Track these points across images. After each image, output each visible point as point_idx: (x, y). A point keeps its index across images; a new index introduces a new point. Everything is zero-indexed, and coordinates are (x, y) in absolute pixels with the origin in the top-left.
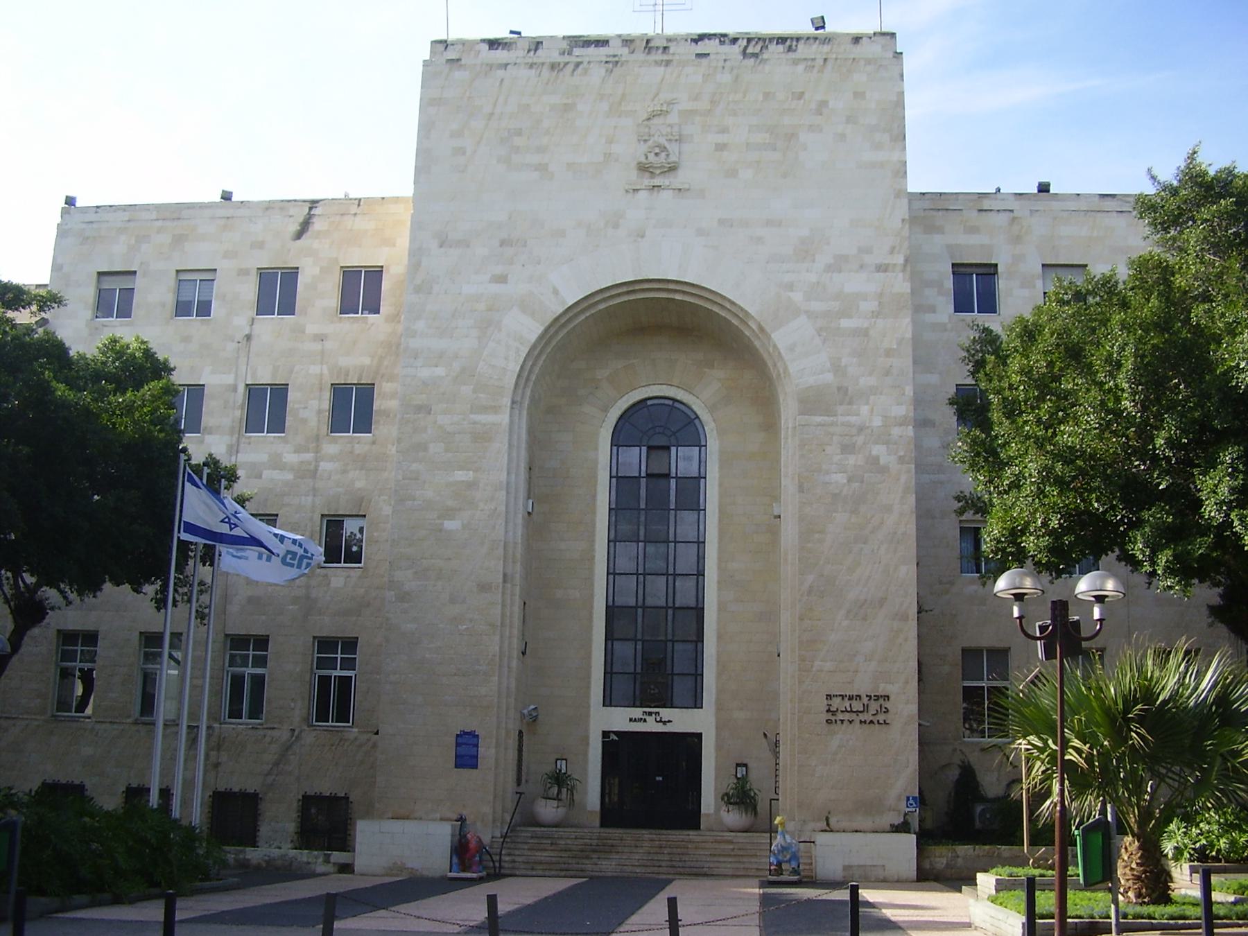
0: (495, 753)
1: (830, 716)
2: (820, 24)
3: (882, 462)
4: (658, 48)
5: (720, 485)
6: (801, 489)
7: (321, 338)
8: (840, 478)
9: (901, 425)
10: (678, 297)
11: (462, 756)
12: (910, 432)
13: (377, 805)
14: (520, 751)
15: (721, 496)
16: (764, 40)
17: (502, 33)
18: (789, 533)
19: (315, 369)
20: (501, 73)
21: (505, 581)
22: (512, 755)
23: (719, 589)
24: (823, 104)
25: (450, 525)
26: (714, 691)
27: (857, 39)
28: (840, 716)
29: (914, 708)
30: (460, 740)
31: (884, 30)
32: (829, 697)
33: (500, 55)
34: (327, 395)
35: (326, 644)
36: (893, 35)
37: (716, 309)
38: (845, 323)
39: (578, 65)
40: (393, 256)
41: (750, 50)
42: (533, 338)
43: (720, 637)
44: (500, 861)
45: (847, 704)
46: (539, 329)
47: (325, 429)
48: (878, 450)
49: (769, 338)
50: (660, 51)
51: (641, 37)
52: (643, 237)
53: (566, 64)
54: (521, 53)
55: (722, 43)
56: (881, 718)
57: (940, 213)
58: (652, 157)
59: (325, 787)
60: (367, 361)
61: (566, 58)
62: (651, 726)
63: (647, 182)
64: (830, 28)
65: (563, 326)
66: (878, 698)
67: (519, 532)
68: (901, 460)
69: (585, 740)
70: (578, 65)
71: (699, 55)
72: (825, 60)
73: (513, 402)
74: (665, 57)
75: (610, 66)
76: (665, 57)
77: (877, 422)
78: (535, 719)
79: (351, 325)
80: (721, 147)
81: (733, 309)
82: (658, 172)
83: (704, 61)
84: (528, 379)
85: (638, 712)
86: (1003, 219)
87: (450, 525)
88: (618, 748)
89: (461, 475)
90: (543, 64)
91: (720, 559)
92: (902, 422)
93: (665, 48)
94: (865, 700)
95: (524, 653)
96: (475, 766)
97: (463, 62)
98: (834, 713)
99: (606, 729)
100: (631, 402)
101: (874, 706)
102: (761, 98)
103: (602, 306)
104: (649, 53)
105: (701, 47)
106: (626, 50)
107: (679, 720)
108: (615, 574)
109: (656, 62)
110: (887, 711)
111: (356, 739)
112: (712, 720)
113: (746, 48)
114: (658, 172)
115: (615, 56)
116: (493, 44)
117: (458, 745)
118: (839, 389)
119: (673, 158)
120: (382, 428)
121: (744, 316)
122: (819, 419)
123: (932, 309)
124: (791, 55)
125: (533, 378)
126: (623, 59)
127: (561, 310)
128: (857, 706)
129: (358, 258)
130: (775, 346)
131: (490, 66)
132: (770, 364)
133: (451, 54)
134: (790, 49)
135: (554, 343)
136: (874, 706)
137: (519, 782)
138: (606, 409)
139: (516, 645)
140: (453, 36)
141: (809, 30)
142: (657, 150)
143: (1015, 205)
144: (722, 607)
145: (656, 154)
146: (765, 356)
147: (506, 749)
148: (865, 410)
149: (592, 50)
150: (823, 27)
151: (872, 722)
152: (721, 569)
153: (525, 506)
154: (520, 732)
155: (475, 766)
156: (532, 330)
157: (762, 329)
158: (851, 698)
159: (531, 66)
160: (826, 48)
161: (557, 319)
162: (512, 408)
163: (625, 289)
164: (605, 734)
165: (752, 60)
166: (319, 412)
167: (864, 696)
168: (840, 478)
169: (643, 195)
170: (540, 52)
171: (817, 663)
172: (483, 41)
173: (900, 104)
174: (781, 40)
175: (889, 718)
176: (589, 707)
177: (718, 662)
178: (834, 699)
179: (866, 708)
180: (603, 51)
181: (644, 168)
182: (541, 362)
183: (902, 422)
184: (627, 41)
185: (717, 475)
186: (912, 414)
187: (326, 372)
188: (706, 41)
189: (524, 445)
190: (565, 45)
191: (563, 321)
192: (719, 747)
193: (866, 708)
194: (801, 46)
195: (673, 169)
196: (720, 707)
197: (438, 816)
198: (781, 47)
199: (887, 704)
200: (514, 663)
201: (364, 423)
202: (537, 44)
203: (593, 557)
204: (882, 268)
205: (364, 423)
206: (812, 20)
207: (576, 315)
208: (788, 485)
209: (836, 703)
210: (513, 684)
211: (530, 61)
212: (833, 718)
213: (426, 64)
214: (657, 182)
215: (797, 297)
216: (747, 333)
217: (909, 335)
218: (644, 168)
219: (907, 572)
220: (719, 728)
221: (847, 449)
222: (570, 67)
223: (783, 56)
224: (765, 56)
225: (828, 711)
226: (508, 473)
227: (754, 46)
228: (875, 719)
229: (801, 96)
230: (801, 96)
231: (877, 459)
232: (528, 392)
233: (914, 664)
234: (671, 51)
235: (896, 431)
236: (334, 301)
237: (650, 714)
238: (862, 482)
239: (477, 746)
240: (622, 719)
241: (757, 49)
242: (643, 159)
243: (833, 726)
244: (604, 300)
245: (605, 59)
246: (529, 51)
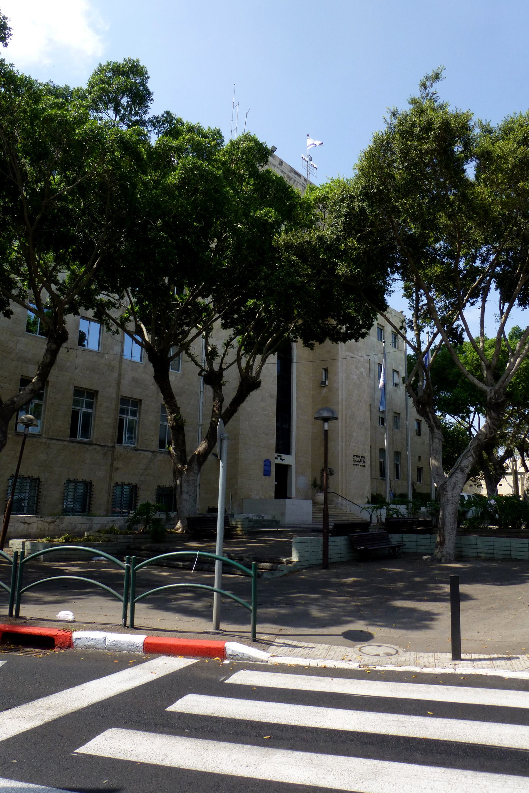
8: (355, 377)
13: (239, 492)
15: (298, 372)
28: (356, 463)
32: (354, 456)
43: (297, 428)
48: (362, 370)
56: (364, 464)
117: (265, 465)
144: (298, 415)
158: (359, 457)
192: (297, 472)
196: (297, 457)
220: (297, 463)
231: (362, 373)
239: (270, 466)
243: (355, 466)
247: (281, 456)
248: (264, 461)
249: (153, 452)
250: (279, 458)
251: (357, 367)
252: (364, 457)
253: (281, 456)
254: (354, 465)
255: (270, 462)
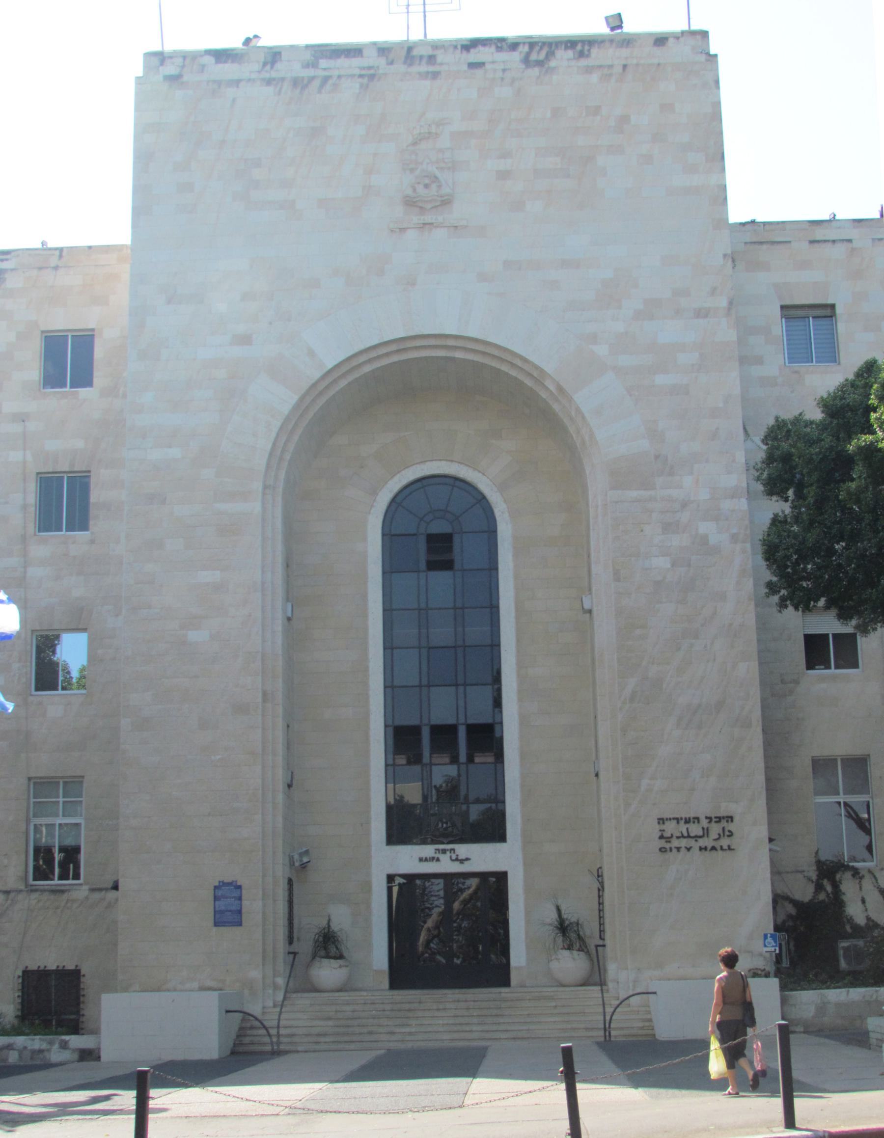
0: (262, 908)
1: (662, 844)
2: (616, 22)
3: (713, 540)
4: (421, 57)
5: (516, 577)
6: (617, 577)
7: (22, 418)
8: (662, 563)
9: (732, 497)
10: (459, 355)
11: (222, 912)
12: (743, 504)
14: (290, 903)
16: (550, 44)
17: (235, 43)
18: (605, 630)
19: (16, 456)
20: (231, 92)
21: (265, 700)
22: (282, 907)
23: (520, 700)
24: (624, 119)
25: (194, 636)
26: (519, 821)
27: (661, 40)
29: (762, 831)
30: (219, 893)
31: (693, 28)
32: (661, 821)
33: (229, 70)
34: (32, 487)
35: (42, 786)
36: (704, 34)
37: (504, 368)
38: (660, 380)
39: (326, 79)
40: (108, 318)
41: (534, 57)
42: (286, 409)
43: (523, 756)
44: (278, 1035)
45: (683, 828)
46: (296, 398)
47: (31, 528)
48: (706, 528)
49: (570, 400)
50: (424, 61)
51: (400, 45)
52: (414, 284)
53: (312, 79)
54: (256, 67)
55: (499, 49)
57: (765, 247)
58: (421, 190)
59: (50, 959)
60: (80, 444)
61: (311, 72)
62: (446, 866)
63: (416, 219)
64: (629, 27)
65: (321, 393)
66: (719, 819)
67: (279, 640)
68: (734, 538)
69: (367, 887)
70: (326, 79)
71: (472, 66)
72: (625, 67)
73: (265, 487)
74: (431, 69)
75: (365, 80)
76: (431, 69)
77: (704, 495)
78: (304, 866)
79: (56, 402)
80: (504, 175)
81: (526, 367)
82: (429, 206)
83: (479, 72)
84: (281, 459)
85: (428, 850)
86: (839, 251)
87: (194, 636)
88: (407, 894)
89: (207, 576)
90: (283, 79)
91: (520, 665)
92: (733, 495)
93: (431, 59)
94: (704, 823)
95: (290, 786)
96: (240, 924)
97: (185, 78)
98: (668, 839)
99: (392, 871)
100: (405, 482)
101: (715, 829)
102: (549, 115)
103: (368, 369)
104: (411, 65)
105: (474, 56)
106: (382, 61)
107: (480, 857)
108: (393, 687)
109: (420, 74)
110: (731, 834)
111: (87, 898)
112: (520, 855)
113: (528, 55)
114: (429, 206)
115: (370, 68)
116: (221, 56)
117: (216, 898)
118: (657, 457)
119: (446, 190)
120: (99, 524)
121: (539, 376)
122: (634, 494)
123: (759, 361)
124: (583, 62)
125: (288, 456)
126: (381, 71)
127: (317, 375)
128: (695, 829)
129: (62, 320)
130: (578, 410)
131: (219, 83)
132: (572, 430)
133: (170, 69)
134: (581, 55)
135: (311, 414)
136: (715, 829)
137: (291, 941)
138: (374, 492)
139: (280, 775)
140: (169, 47)
141: (603, 29)
142: (427, 181)
143: (853, 234)
144: (524, 720)
145: (427, 186)
146: (566, 421)
147: (275, 901)
148: (688, 481)
149: (342, 62)
150: (620, 27)
151: (714, 848)
152: (522, 679)
153: (284, 611)
154: (290, 882)
155: (240, 924)
156: (284, 399)
157: (560, 389)
158: (687, 821)
159: (269, 82)
160: (625, 52)
161: (314, 386)
162: (264, 494)
163: (394, 347)
164: (390, 878)
165: (536, 70)
166: (25, 507)
167: (703, 819)
168: (662, 563)
169: (411, 234)
170: (278, 66)
171: (645, 782)
172: (209, 52)
173: (716, 116)
174: (571, 43)
175: (734, 842)
176: (369, 846)
177: (522, 786)
178: (667, 823)
179: (706, 832)
180: (356, 62)
181: (410, 203)
182: (296, 438)
183: (733, 495)
184: (384, 50)
185: (511, 565)
186: (744, 485)
187: (29, 458)
188: (481, 48)
189: (279, 537)
190: (308, 56)
191: (321, 387)
192: (528, 888)
193: (706, 832)
194: (594, 51)
195: (446, 202)
196: (527, 841)
197: (195, 985)
198: (570, 53)
199: (731, 827)
200: (280, 798)
201: (80, 519)
202: (274, 55)
203: (366, 669)
204: (701, 313)
205: (80, 519)
206: (607, 19)
207: (335, 381)
208: (601, 573)
209: (670, 828)
210: (280, 825)
211: (267, 76)
212: (668, 846)
213: (139, 81)
214: (428, 218)
215: (602, 350)
216: (544, 395)
217: (737, 391)
218: (410, 203)
219: (748, 670)
220: (528, 864)
221: (668, 528)
222: (317, 83)
223: (573, 63)
224: (553, 63)
225: (661, 837)
226: (263, 572)
227: (539, 52)
228: (717, 845)
229: (597, 110)
230: (597, 110)
231: (704, 539)
232: (282, 475)
233: (760, 778)
234: (440, 59)
235: (727, 505)
236: (34, 373)
237: (444, 851)
238: (689, 565)
239: (240, 898)
240: (410, 859)
241: (542, 56)
242: (409, 192)
244: (370, 361)
245: (357, 72)
246: (265, 64)
247: (453, 850)
248: (215, 887)
249: (7, 892)
250: (445, 858)
251: (668, 528)
252: (730, 819)
253: (453, 850)
254: (662, 850)
255: (240, 887)
